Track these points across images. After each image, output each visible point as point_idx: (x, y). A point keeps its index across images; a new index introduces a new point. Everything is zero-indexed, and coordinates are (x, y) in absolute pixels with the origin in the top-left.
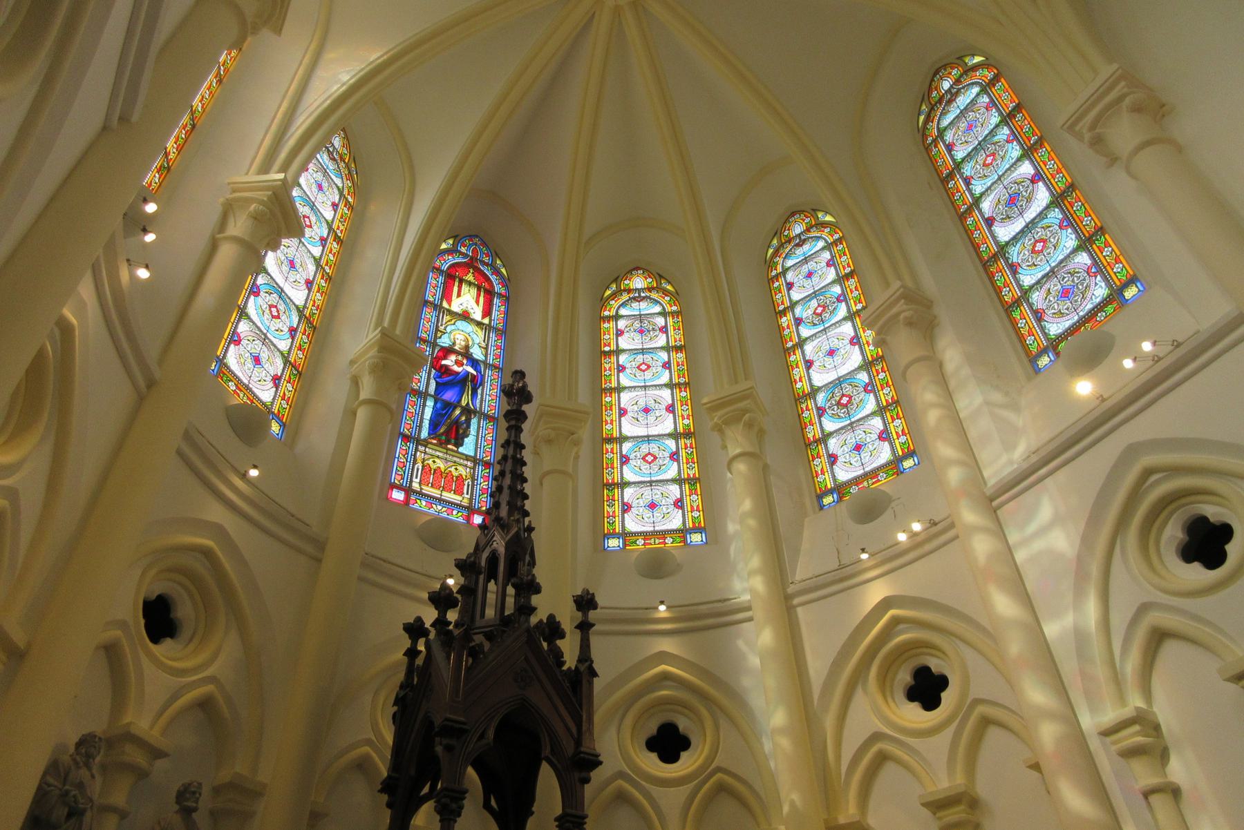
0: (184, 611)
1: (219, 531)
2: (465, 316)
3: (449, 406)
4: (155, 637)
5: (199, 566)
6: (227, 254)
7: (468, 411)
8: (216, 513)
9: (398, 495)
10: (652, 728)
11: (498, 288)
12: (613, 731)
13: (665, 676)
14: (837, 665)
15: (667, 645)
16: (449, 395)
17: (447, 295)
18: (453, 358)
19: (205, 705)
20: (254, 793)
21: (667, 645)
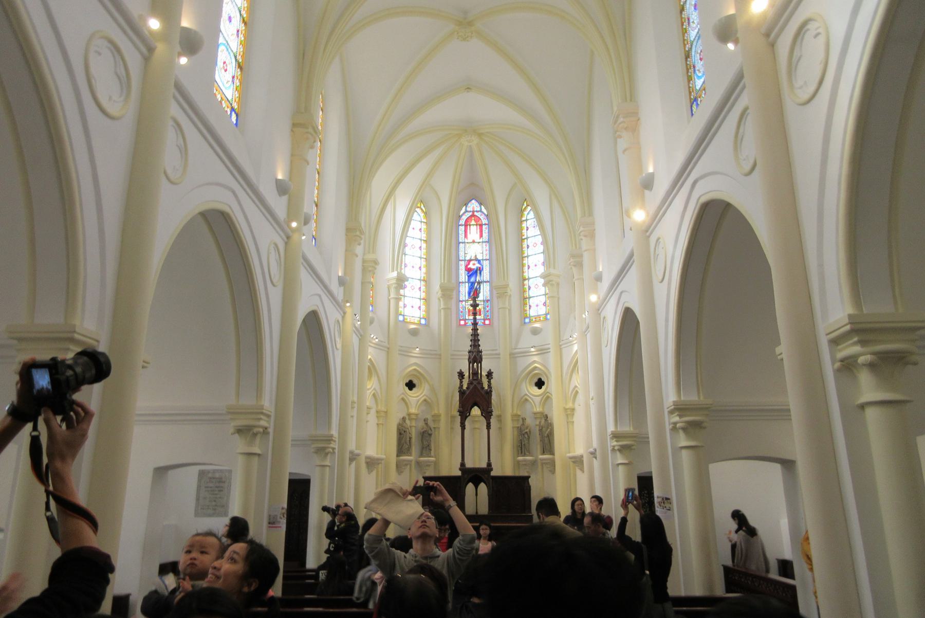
0: (415, 382)
1: (415, 364)
2: (474, 242)
3: (473, 284)
4: (411, 389)
5: (415, 373)
6: (392, 302)
7: (479, 283)
8: (413, 361)
9: (462, 323)
10: (536, 380)
11: (485, 221)
12: (524, 384)
13: (536, 367)
14: (569, 366)
15: (536, 358)
16: (472, 279)
17: (466, 236)
18: (472, 263)
19: (425, 400)
20: (440, 416)
21: (536, 358)
